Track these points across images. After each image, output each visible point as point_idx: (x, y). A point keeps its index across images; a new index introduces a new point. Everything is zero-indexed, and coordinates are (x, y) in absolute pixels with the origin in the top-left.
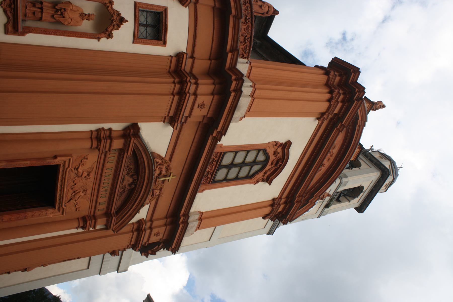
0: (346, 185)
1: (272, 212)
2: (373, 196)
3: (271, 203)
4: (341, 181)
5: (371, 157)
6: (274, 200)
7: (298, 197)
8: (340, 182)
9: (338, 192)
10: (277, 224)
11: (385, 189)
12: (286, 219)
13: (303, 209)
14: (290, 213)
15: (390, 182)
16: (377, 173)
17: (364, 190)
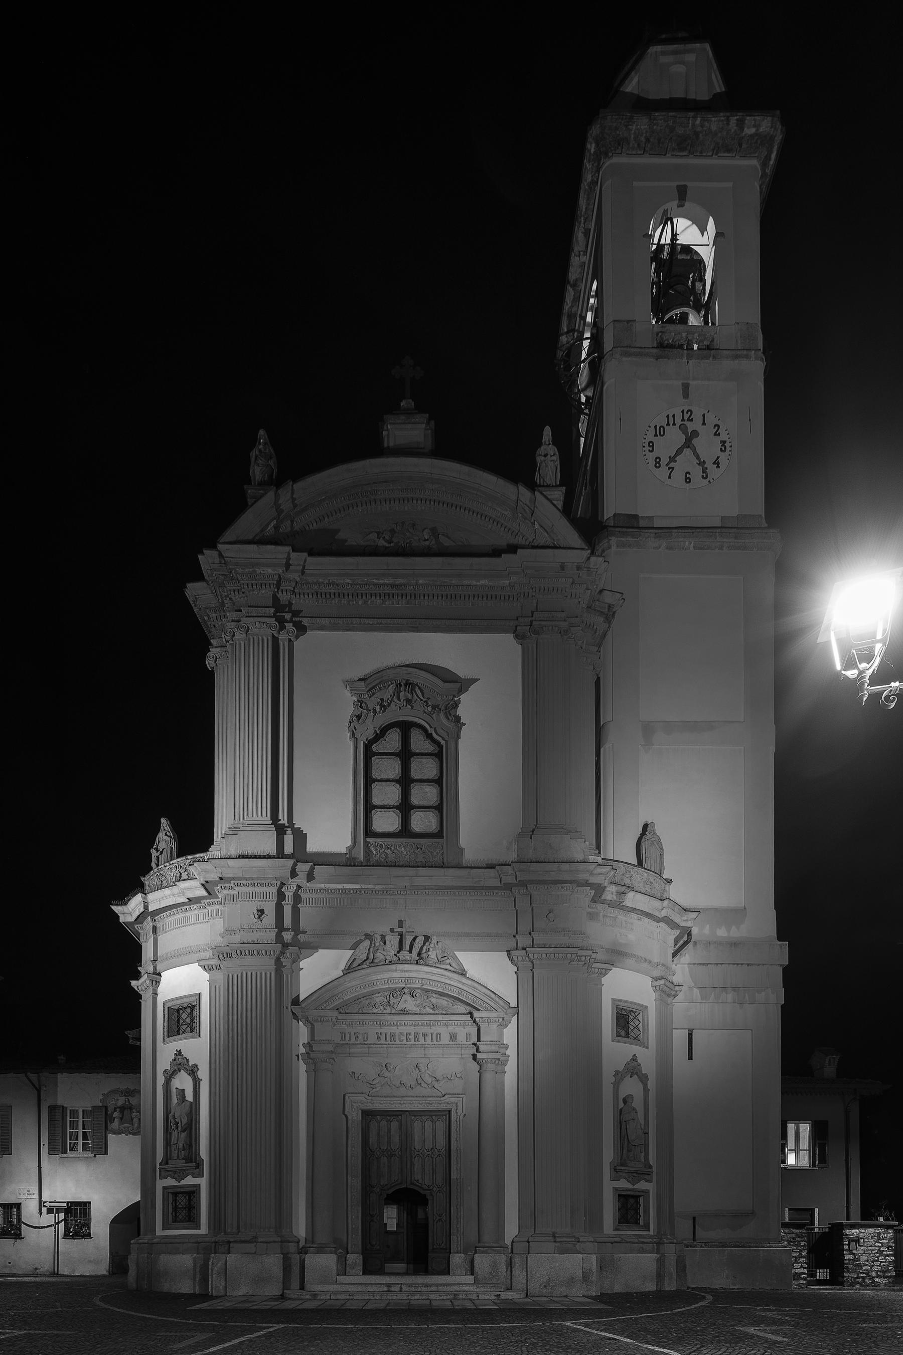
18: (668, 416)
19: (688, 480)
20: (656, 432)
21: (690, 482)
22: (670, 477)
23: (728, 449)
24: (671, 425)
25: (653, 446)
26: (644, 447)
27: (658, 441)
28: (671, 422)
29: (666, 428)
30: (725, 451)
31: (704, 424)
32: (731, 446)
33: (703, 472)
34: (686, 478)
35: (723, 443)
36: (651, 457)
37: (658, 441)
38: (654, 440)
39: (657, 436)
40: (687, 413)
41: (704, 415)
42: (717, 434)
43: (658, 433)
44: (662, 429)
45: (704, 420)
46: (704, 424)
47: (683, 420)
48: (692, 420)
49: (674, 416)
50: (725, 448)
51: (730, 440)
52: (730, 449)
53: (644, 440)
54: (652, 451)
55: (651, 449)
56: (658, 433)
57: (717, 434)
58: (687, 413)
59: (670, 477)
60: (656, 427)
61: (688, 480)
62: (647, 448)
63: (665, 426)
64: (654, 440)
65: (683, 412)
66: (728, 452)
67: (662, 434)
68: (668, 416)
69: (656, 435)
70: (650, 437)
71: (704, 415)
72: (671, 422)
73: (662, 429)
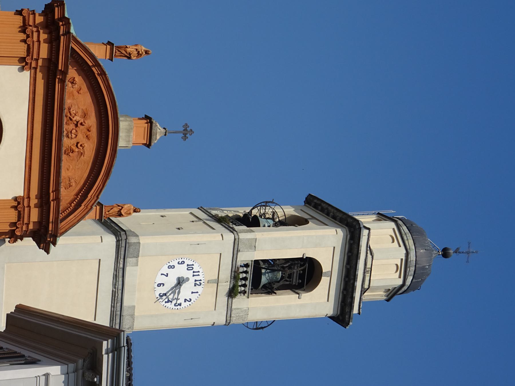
0: (255, 247)
1: (20, 218)
2: (352, 282)
3: (15, 204)
4: (237, 237)
5: (335, 211)
6: (16, 199)
7: (53, 192)
8: (235, 239)
9: (247, 266)
10: (119, 313)
11: (400, 277)
12: (50, 232)
13: (75, 216)
14: (51, 220)
15: (402, 259)
16: (336, 230)
17: (326, 268)
18: (199, 272)
19: (159, 285)
20: (190, 265)
21: (158, 286)
22: (162, 274)
23: (176, 307)
24: (193, 274)
25: (181, 263)
26: (182, 259)
27: (185, 266)
28: (195, 274)
29: (192, 271)
30: (175, 305)
31: (192, 293)
32: (178, 309)
33: (163, 294)
34: (160, 284)
35: (180, 304)
36: (175, 263)
37: (185, 266)
38: (185, 264)
39: (187, 266)
40: (199, 283)
41: (197, 292)
42: (185, 300)
43: (189, 266)
44: (192, 268)
45: (194, 293)
46: (192, 293)
47: (196, 281)
48: (195, 286)
49: (199, 275)
50: (177, 306)
51: (181, 308)
52: (176, 309)
53: (185, 259)
54: (178, 263)
55: (180, 263)
56: (189, 266)
57: (185, 300)
58: (199, 283)
59: (162, 274)
60: (193, 265)
61: (159, 285)
62: (181, 261)
63: (193, 270)
64: (185, 264)
65: (201, 280)
66: (174, 307)
67: (189, 269)
68: (199, 272)
69: (188, 265)
70: (187, 262)
71: (197, 292)
72: (195, 274)
73: (192, 268)
